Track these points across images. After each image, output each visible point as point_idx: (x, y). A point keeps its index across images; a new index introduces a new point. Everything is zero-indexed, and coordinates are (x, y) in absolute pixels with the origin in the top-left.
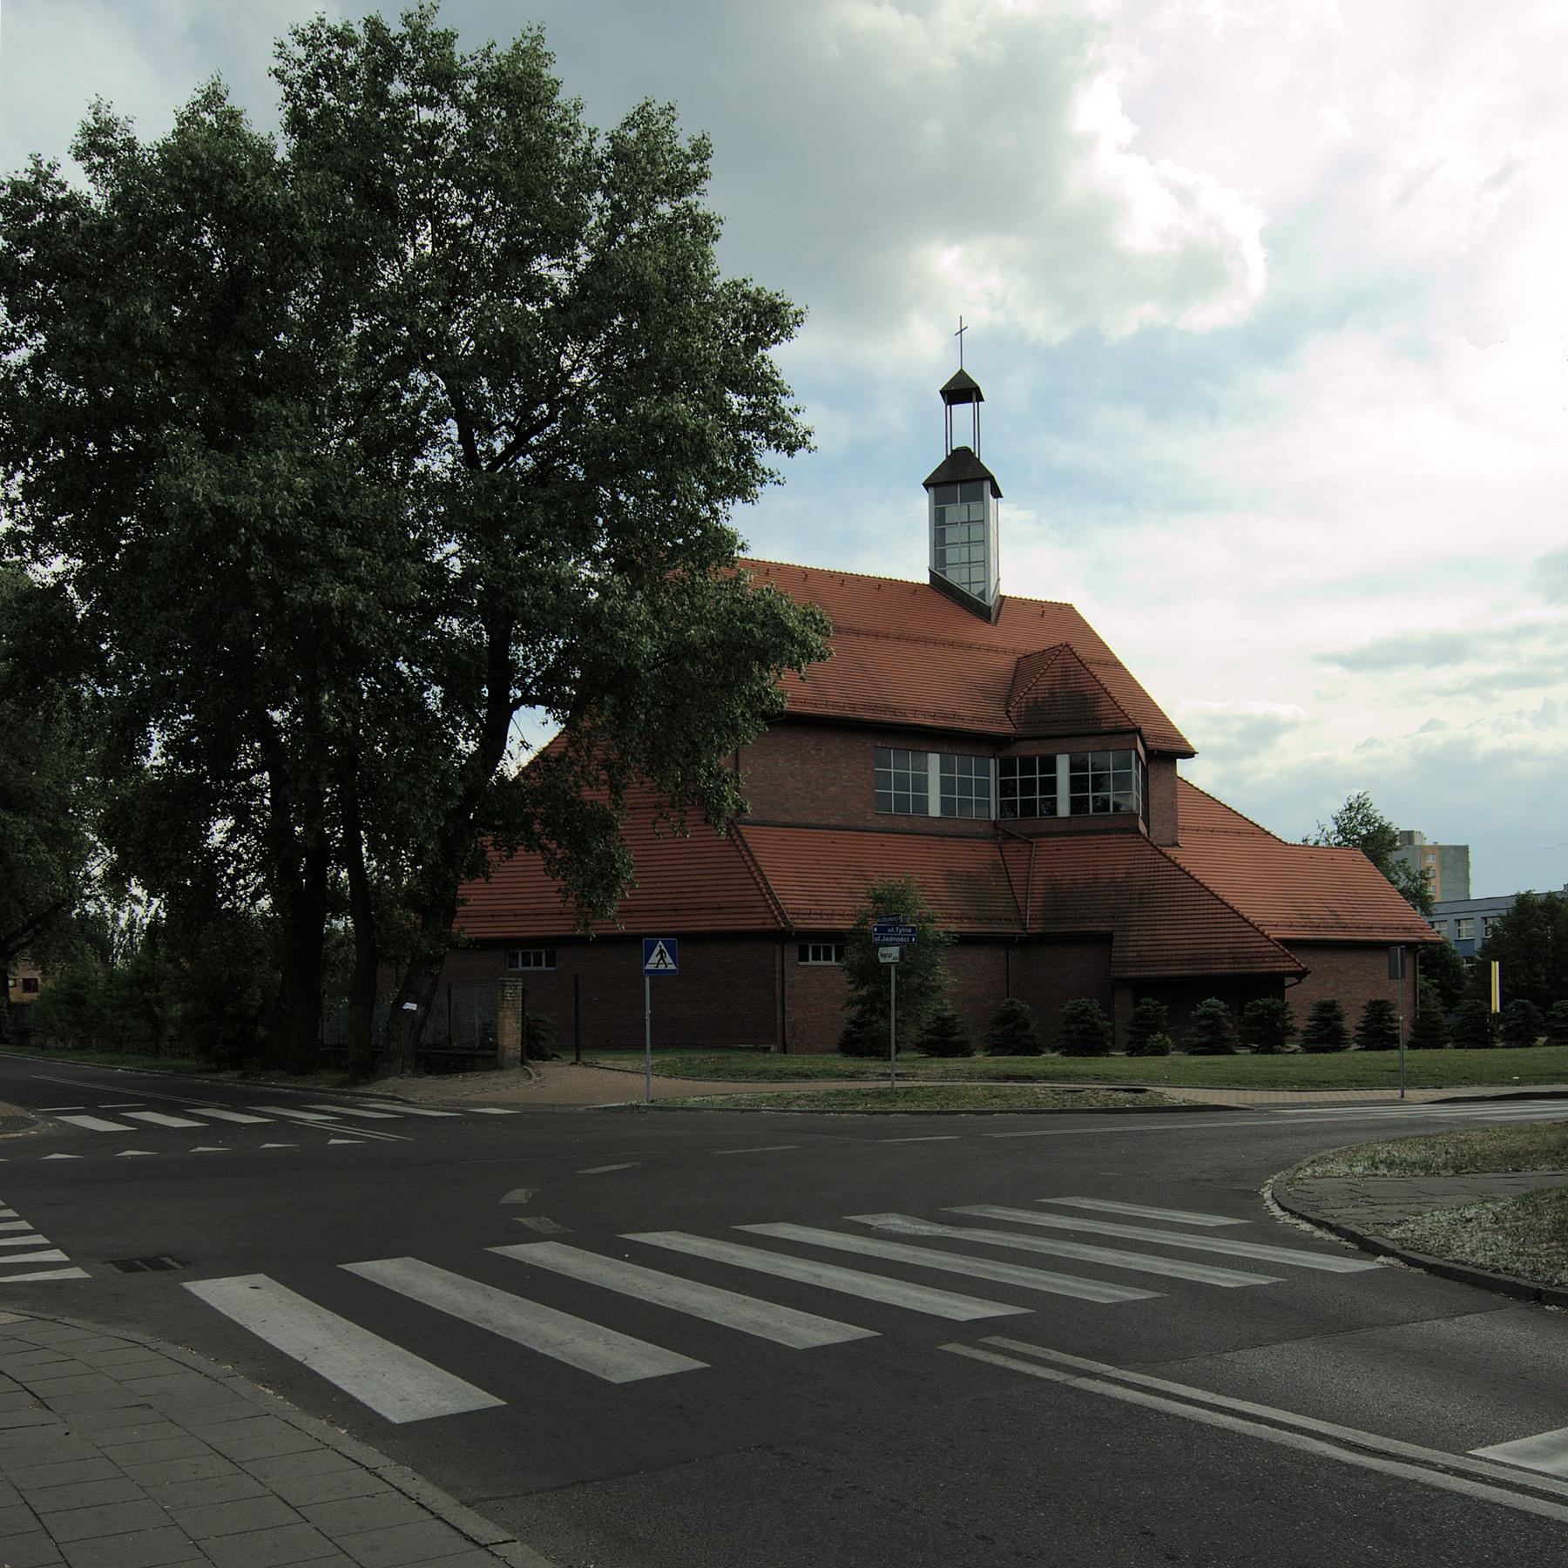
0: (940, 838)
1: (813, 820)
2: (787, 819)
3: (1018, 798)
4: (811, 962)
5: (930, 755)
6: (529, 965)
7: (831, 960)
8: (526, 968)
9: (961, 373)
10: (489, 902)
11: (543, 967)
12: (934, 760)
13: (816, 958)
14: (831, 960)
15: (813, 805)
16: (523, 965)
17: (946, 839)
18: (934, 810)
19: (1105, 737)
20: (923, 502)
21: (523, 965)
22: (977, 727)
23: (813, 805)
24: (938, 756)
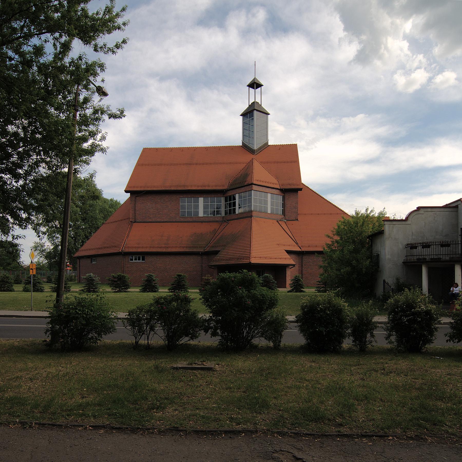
0: (201, 223)
1: (159, 220)
2: (150, 220)
3: (209, 210)
4: (134, 261)
5: (199, 198)
6: (137, 260)
7: (140, 260)
8: (136, 261)
9: (255, 79)
10: (273, 245)
11: (141, 261)
12: (201, 200)
13: (136, 259)
14: (140, 260)
15: (158, 216)
16: (135, 260)
17: (203, 223)
18: (201, 214)
19: (246, 187)
20: (240, 120)
21: (135, 260)
22: (214, 188)
23: (158, 216)
24: (203, 198)
